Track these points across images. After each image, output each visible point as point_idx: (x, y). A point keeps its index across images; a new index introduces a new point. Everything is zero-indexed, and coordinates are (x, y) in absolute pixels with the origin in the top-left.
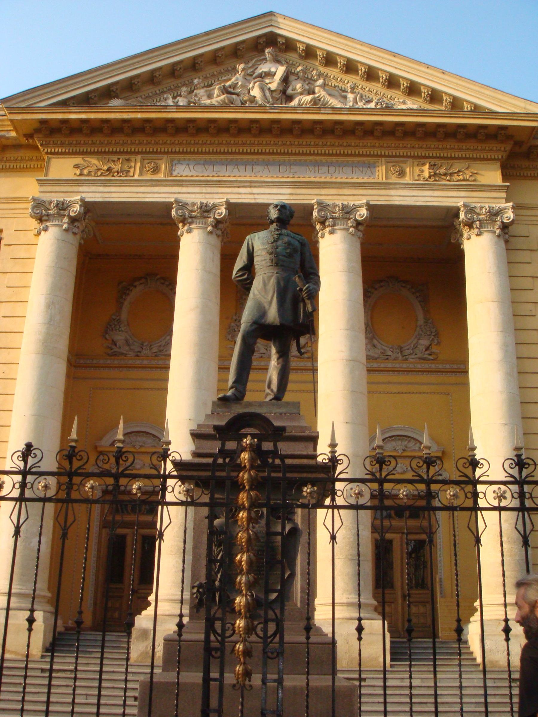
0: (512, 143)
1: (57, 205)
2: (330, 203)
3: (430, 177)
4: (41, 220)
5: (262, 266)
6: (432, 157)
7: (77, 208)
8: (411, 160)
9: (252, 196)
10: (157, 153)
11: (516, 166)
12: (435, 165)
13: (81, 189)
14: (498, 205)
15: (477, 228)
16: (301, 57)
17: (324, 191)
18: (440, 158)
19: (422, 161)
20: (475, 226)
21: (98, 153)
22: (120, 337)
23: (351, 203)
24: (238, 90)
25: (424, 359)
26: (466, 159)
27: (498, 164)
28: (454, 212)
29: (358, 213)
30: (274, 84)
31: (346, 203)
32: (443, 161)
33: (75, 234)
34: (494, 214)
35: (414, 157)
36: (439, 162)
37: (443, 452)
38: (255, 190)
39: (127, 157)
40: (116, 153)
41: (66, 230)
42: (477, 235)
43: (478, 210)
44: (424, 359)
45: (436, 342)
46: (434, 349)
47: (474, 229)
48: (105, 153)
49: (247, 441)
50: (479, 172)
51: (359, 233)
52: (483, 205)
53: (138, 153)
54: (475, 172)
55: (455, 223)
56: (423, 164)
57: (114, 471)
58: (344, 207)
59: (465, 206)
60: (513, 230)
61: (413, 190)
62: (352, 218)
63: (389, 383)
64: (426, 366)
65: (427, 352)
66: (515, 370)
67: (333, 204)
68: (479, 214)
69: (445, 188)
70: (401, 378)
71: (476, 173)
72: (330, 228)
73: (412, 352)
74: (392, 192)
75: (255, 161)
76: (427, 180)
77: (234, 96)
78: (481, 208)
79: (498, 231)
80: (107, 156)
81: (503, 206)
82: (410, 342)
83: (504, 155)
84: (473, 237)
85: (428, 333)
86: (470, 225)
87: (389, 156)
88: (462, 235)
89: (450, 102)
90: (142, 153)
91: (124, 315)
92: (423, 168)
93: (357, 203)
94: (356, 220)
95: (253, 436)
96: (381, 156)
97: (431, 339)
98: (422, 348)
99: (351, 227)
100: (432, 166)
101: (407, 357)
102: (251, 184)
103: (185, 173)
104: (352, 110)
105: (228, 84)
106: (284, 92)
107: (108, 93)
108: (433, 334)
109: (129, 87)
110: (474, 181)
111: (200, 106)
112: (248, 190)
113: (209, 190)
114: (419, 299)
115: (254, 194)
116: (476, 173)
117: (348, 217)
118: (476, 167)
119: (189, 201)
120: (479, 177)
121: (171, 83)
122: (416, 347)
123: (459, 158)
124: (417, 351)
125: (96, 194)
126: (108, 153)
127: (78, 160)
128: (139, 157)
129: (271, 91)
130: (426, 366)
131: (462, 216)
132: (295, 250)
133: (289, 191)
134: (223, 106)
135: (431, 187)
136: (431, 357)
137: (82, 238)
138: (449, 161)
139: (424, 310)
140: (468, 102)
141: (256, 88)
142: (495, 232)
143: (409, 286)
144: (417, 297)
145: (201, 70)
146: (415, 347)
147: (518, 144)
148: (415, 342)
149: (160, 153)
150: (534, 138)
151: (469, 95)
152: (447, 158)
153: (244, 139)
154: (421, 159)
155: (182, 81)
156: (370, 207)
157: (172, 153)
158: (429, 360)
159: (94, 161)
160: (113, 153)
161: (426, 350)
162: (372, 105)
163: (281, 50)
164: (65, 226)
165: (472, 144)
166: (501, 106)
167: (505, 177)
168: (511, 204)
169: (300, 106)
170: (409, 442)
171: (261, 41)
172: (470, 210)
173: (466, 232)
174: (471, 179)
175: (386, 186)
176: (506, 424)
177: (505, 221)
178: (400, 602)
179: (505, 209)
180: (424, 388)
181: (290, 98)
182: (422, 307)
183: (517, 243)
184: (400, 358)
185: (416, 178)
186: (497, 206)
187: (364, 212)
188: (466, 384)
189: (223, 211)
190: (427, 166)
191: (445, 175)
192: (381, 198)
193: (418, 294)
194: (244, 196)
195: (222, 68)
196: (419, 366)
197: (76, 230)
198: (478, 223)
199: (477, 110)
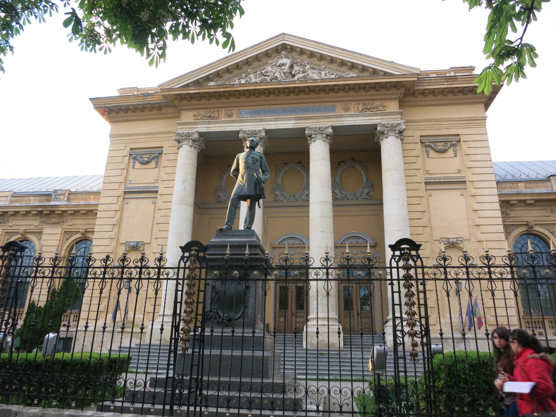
1: (186, 135)
2: (314, 126)
4: (179, 141)
6: (362, 100)
7: (196, 136)
8: (353, 102)
9: (276, 126)
10: (232, 107)
13: (197, 126)
16: (299, 55)
17: (310, 121)
19: (358, 102)
21: (204, 108)
22: (221, 194)
23: (324, 126)
24: (268, 74)
25: (366, 199)
26: (381, 99)
28: (375, 127)
30: (286, 68)
33: (195, 148)
35: (355, 101)
36: (367, 102)
37: (376, 244)
38: (278, 123)
39: (218, 110)
40: (213, 108)
41: (191, 146)
46: (372, 194)
48: (208, 108)
49: (193, 252)
53: (223, 107)
57: (140, 266)
60: (405, 133)
61: (354, 118)
63: (349, 211)
64: (367, 202)
66: (406, 203)
69: (370, 115)
70: (355, 208)
74: (344, 119)
77: (267, 77)
80: (209, 110)
81: (399, 122)
87: (342, 101)
90: (225, 107)
91: (223, 184)
93: (326, 126)
95: (195, 250)
96: (339, 101)
102: (276, 120)
103: (245, 116)
104: (323, 80)
105: (263, 72)
106: (291, 73)
107: (208, 79)
109: (218, 75)
111: (250, 83)
112: (275, 123)
113: (256, 123)
119: (247, 129)
121: (236, 72)
123: (377, 100)
124: (362, 195)
125: (203, 128)
126: (209, 108)
127: (195, 112)
128: (223, 109)
129: (284, 73)
130: (367, 202)
132: (257, 161)
133: (293, 122)
134: (262, 82)
137: (199, 149)
141: (276, 72)
145: (251, 65)
146: (362, 193)
149: (233, 107)
153: (272, 98)
155: (242, 71)
156: (333, 128)
157: (238, 106)
158: (368, 199)
159: (202, 112)
160: (211, 108)
162: (333, 77)
163: (289, 52)
164: (191, 144)
167: (401, 106)
169: (298, 79)
171: (279, 48)
175: (341, 116)
178: (356, 316)
181: (294, 76)
183: (407, 140)
184: (354, 198)
188: (382, 210)
189: (263, 134)
190: (361, 105)
192: (338, 122)
194: (273, 126)
195: (261, 63)
197: (196, 146)
199: (386, 74)
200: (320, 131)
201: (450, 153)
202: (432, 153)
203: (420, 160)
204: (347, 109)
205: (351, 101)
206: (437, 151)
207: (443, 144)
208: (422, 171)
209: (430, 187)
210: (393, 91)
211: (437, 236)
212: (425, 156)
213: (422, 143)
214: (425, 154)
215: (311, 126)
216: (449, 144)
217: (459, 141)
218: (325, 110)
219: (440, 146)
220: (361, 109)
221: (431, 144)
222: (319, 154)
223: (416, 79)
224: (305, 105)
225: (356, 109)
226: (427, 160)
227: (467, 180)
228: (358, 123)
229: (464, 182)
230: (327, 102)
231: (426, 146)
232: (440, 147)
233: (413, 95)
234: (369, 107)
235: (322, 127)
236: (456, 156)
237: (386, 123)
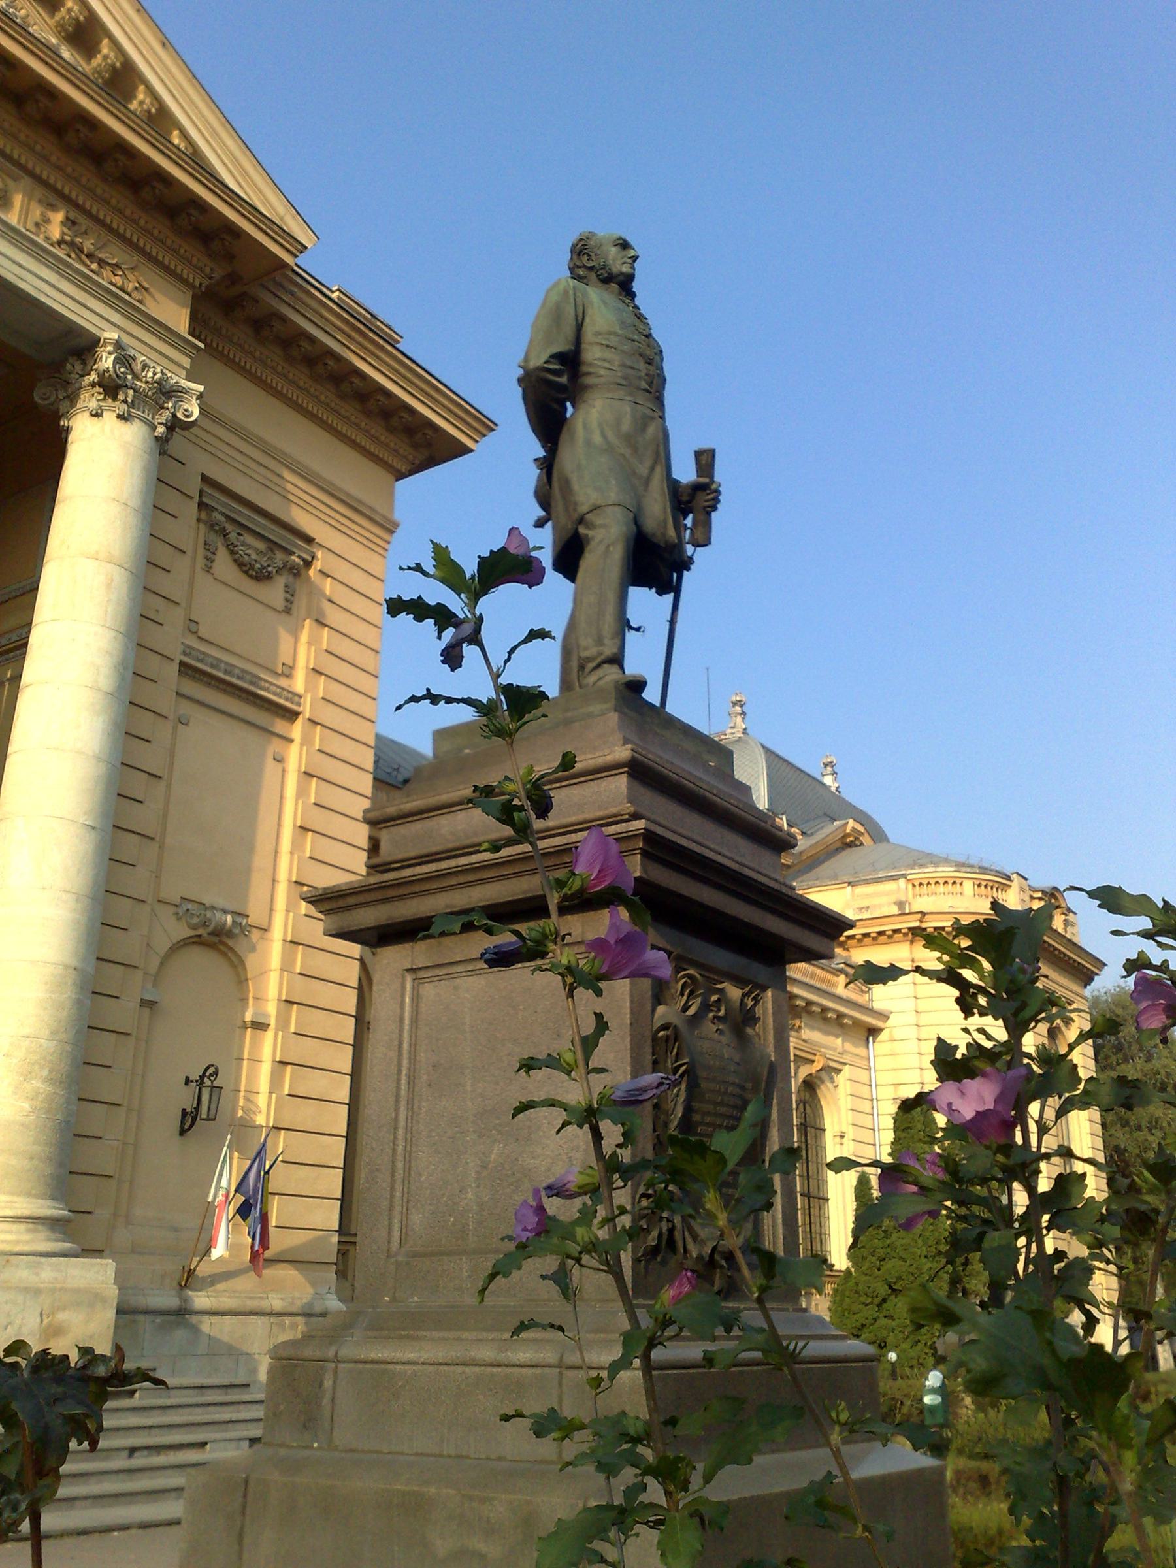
14: (176, 379)
15: (125, 402)
18: (88, 214)
19: (52, 198)
20: (121, 396)
28: (84, 347)
34: (166, 392)
36: (83, 220)
42: (120, 417)
43: (138, 367)
47: (115, 398)
50: (152, 290)
54: (146, 285)
55: (68, 367)
59: (118, 345)
68: (136, 377)
71: (146, 289)
76: (52, 245)
78: (145, 366)
79: (161, 430)
83: (206, 282)
84: (109, 418)
86: (111, 388)
88: (73, 399)
89: (149, 111)
92: (51, 215)
100: (69, 222)
116: (146, 289)
118: (149, 276)
120: (148, 299)
131: (107, 361)
135: (59, 266)
140: (185, 135)
142: (154, 428)
150: (263, 286)
151: (195, 121)
152: (101, 223)
154: (54, 196)
166: (241, 186)
168: (201, 388)
172: (124, 359)
173: (90, 399)
176: (94, 828)
177: (180, 415)
179: (186, 391)
186: (178, 379)
191: (90, 256)
198: (131, 392)
202: (223, 564)
203: (182, 566)
206: (240, 564)
207: (261, 546)
208: (178, 614)
209: (192, 688)
211: (173, 890)
212: (200, 562)
213: (202, 505)
214: (201, 551)
216: (279, 556)
217: (308, 564)
219: (253, 548)
221: (229, 527)
226: (201, 578)
227: (306, 709)
231: (212, 526)
236: (287, 611)
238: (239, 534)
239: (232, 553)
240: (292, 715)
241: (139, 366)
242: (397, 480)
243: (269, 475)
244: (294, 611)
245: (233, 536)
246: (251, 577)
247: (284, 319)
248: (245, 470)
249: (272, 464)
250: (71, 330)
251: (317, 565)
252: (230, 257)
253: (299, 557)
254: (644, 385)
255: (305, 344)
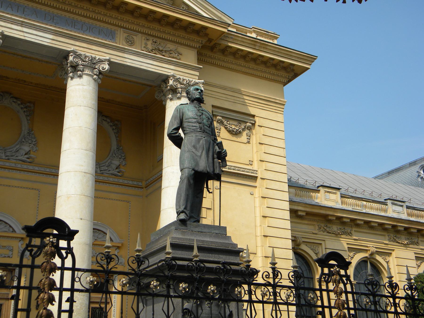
0: (207, 39)
2: (83, 53)
3: (152, 50)
5: (193, 130)
6: (155, 36)
11: (203, 54)
12: (156, 42)
14: (194, 80)
17: (77, 43)
18: (160, 38)
23: (98, 57)
25: (115, 175)
27: (196, 51)
28: (165, 79)
29: (102, 65)
31: (93, 56)
32: (161, 40)
36: (159, 41)
44: (115, 175)
45: (124, 163)
51: (99, 80)
52: (184, 78)
55: (162, 86)
56: (148, 40)
58: (93, 59)
62: (97, 68)
64: (116, 180)
65: (117, 170)
67: (84, 55)
72: (81, 72)
73: (107, 168)
75: (26, 5)
81: (197, 81)
82: (105, 161)
83: (201, 45)
85: (120, 157)
87: (126, 28)
88: (165, 95)
93: (102, 58)
94: (99, 70)
97: (121, 161)
98: (114, 167)
99: (95, 74)
101: (103, 172)
102: (22, 24)
108: (123, 158)
110: (180, 59)
114: (114, 131)
115: (23, 32)
117: (94, 66)
122: (109, 165)
130: (116, 180)
136: (119, 174)
138: (165, 41)
139: (117, 139)
143: (19, 102)
144: (113, 129)
147: (210, 40)
148: (109, 161)
156: (111, 63)
161: (116, 169)
165: (182, 33)
170: (100, 234)
174: (178, 57)
180: (113, 196)
182: (116, 137)
185: (143, 49)
187: (107, 67)
191: (161, 51)
193: (114, 127)
196: (111, 179)
200: (92, 64)
201: (244, 137)
204: (131, 43)
205: (138, 32)
207: (236, 123)
210: (194, 37)
215: (80, 52)
217: (254, 124)
218: (100, 33)
220: (150, 47)
221: (223, 120)
222: (80, 98)
223: (226, 30)
224: (72, 16)
225: (143, 46)
227: (259, 175)
228: (144, 67)
229: (255, 178)
230: (105, 22)
232: (233, 127)
233: (212, 49)
234: (161, 49)
235: (95, 58)
236: (249, 142)
237: (181, 77)
238: (228, 121)
239: (226, 128)
240: (255, 178)
241: (182, 80)
242: (284, 86)
243: (235, 98)
244: (251, 142)
245: (225, 122)
246: (234, 134)
247: (231, 47)
248: (227, 99)
249: (236, 95)
250: (160, 75)
251: (257, 124)
252: (207, 35)
253: (250, 123)
254: (199, 130)
255: (240, 53)
